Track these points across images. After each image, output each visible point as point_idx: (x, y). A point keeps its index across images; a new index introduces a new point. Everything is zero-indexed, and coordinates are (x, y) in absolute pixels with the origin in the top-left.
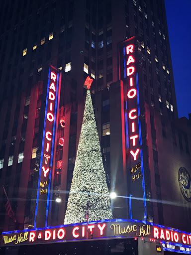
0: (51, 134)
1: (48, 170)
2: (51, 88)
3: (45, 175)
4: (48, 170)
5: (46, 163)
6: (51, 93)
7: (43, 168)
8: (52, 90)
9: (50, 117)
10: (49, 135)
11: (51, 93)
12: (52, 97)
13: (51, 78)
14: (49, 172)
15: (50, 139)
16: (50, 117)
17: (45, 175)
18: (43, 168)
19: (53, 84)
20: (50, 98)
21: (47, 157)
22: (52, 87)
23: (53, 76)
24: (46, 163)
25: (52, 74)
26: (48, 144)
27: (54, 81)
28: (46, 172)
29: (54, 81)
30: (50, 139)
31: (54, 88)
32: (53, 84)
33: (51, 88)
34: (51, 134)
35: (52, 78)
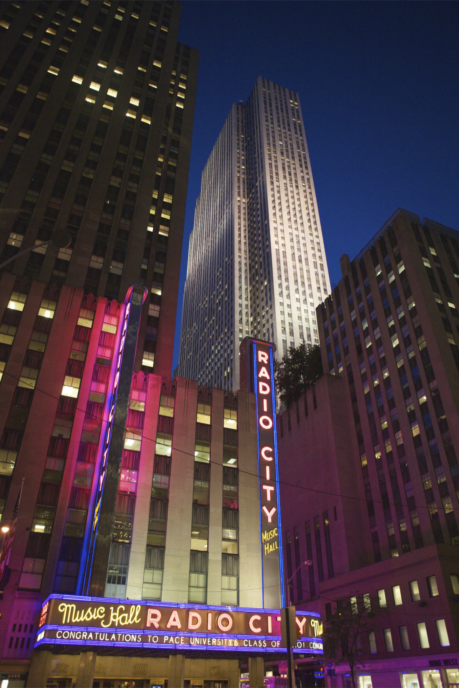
0: (270, 450)
1: (274, 510)
2: (260, 375)
3: (270, 520)
4: (274, 510)
5: (269, 498)
6: (261, 384)
7: (264, 508)
8: (264, 379)
9: (266, 422)
10: (268, 454)
11: (261, 384)
12: (265, 389)
13: (260, 360)
14: (276, 513)
15: (270, 459)
16: (266, 422)
17: (270, 520)
18: (264, 508)
19: (264, 369)
20: (261, 392)
21: (269, 489)
22: (264, 373)
23: (263, 356)
24: (269, 498)
25: (260, 353)
26: (268, 468)
27: (266, 362)
28: (270, 515)
29: (266, 362)
30: (270, 459)
31: (267, 375)
32: (264, 369)
33: (260, 375)
34: (270, 450)
35: (260, 359)
